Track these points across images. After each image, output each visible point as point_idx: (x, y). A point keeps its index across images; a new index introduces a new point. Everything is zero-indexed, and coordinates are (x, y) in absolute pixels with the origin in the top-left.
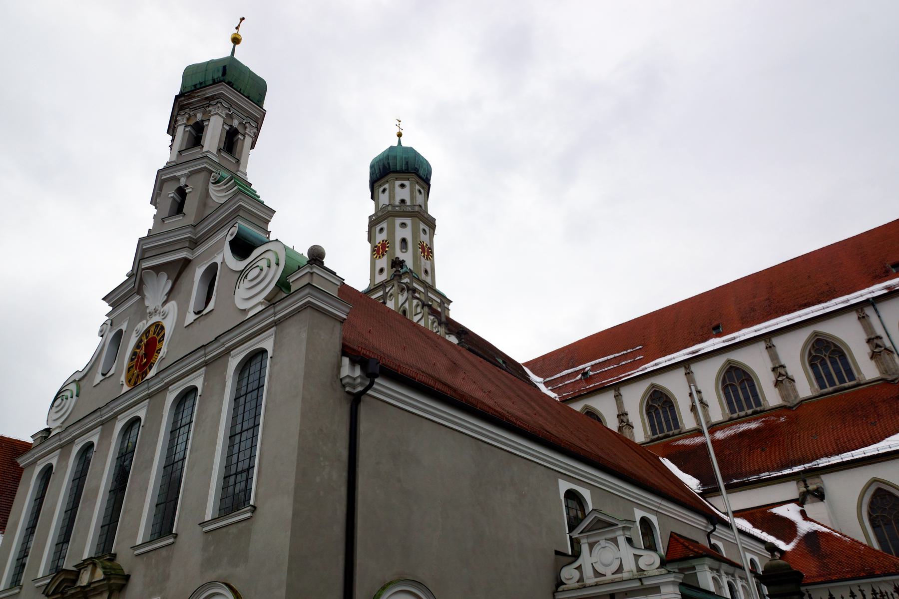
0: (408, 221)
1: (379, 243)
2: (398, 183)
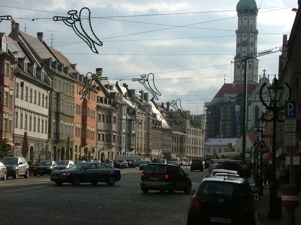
0: (253, 34)
1: (244, 41)
2: (250, 17)
